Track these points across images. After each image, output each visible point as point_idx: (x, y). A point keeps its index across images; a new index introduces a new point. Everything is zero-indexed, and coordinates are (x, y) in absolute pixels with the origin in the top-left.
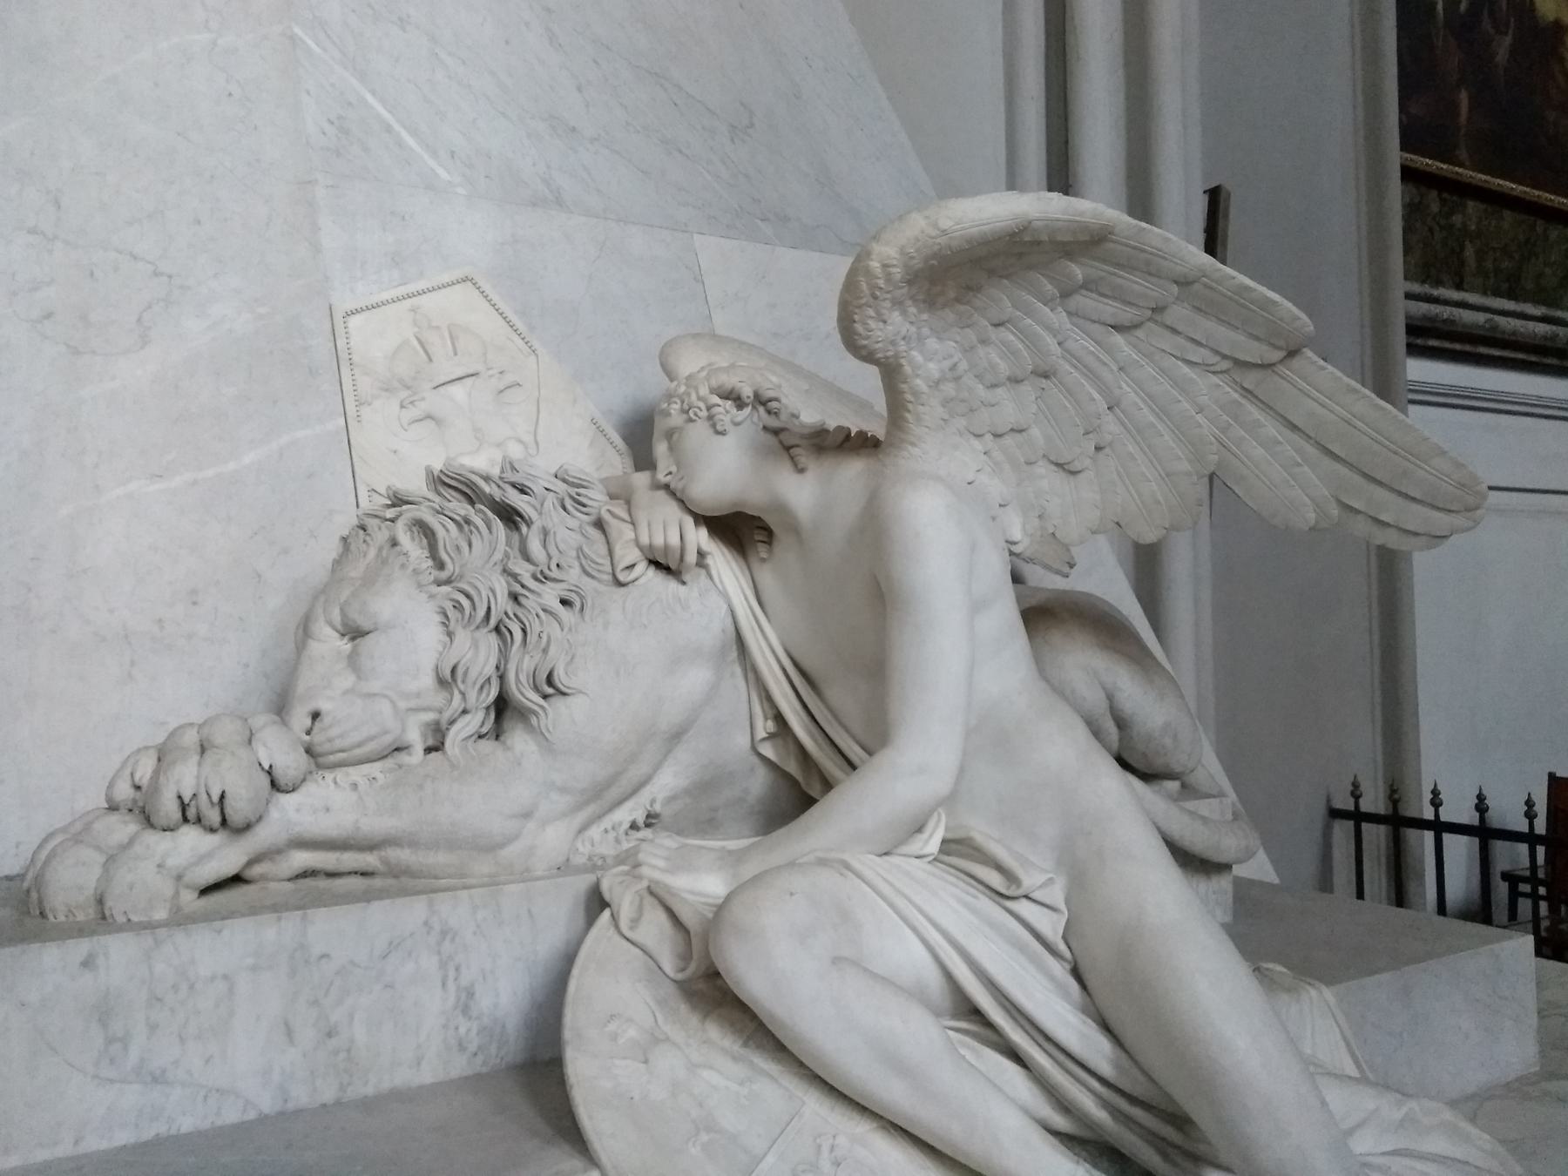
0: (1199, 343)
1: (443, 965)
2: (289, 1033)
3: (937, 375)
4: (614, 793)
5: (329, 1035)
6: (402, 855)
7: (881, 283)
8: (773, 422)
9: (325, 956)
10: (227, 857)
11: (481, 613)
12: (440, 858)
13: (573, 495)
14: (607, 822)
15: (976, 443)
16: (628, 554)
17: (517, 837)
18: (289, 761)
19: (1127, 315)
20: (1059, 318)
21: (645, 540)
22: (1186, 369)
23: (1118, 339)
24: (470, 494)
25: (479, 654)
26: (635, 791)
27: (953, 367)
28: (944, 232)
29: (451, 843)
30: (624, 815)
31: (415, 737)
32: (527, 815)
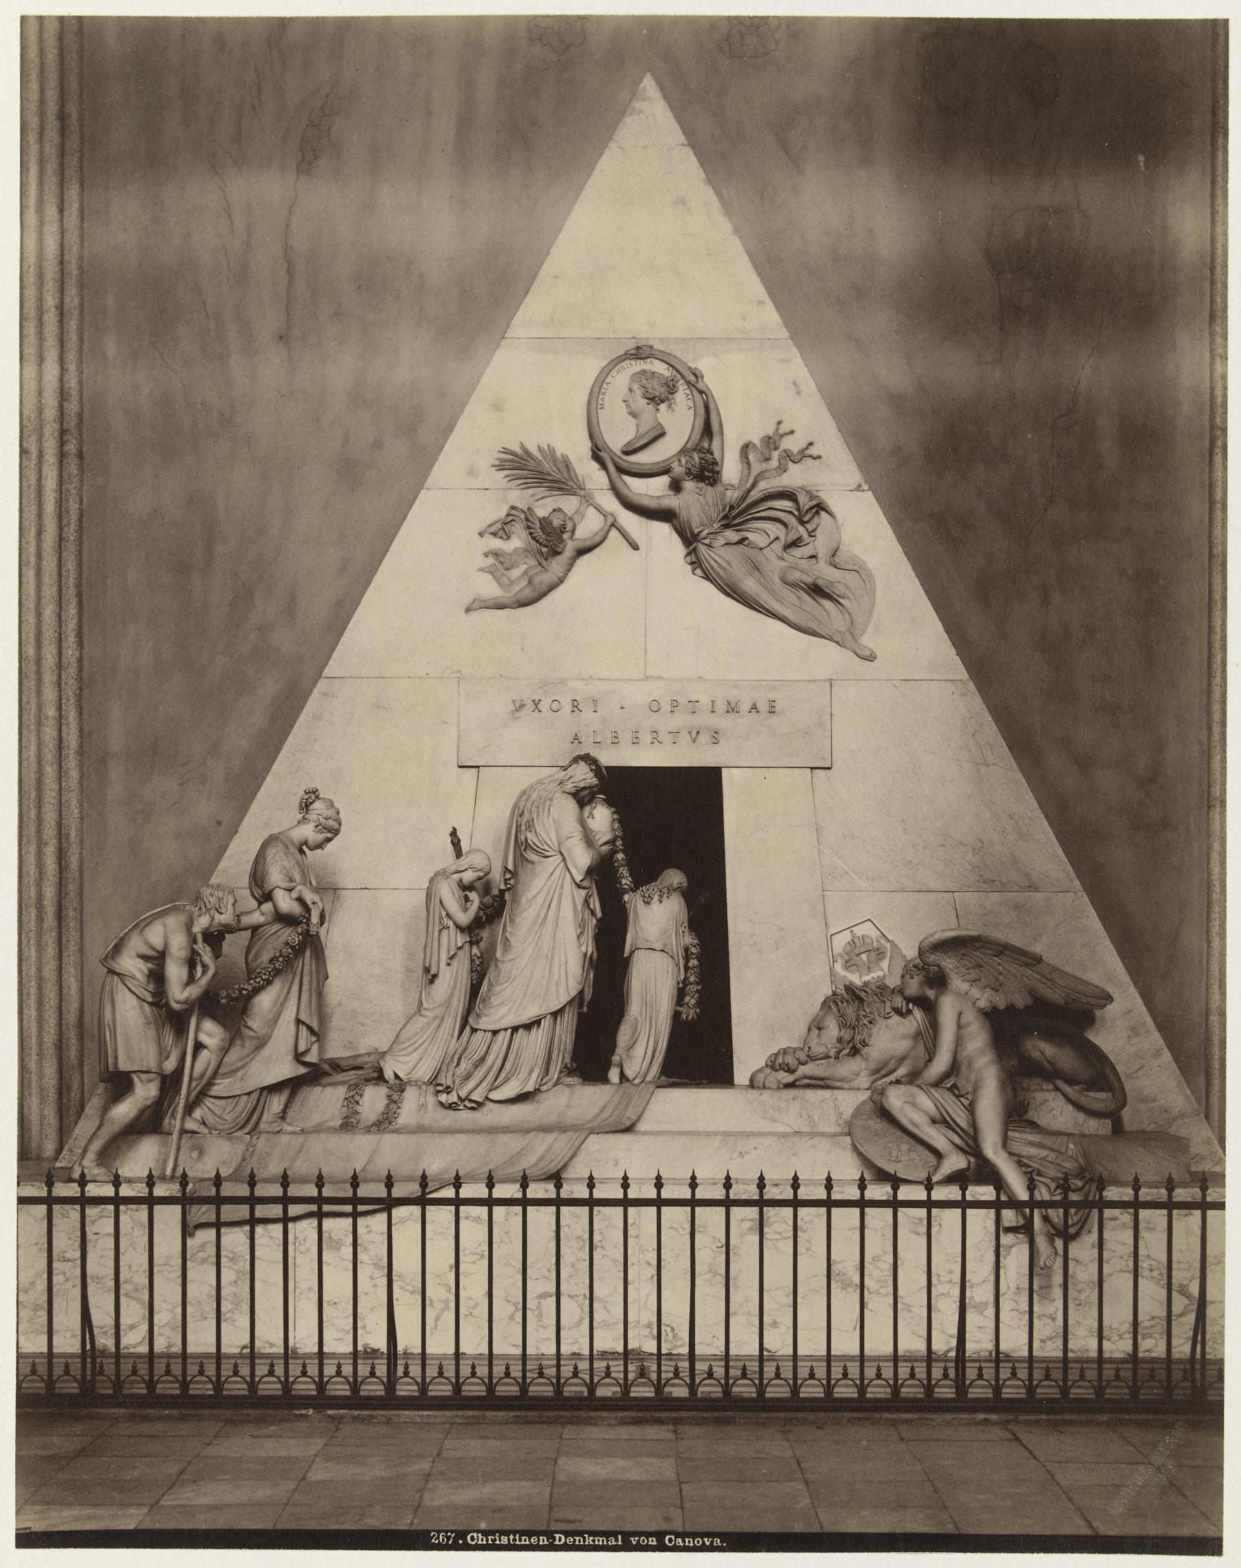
4: (883, 1072)
6: (828, 1082)
12: (838, 1084)
13: (882, 990)
16: (888, 1010)
18: (802, 1056)
24: (853, 991)
25: (846, 1035)
26: (891, 1072)
29: (841, 1080)
30: (887, 1079)
31: (832, 1053)
32: (858, 1075)
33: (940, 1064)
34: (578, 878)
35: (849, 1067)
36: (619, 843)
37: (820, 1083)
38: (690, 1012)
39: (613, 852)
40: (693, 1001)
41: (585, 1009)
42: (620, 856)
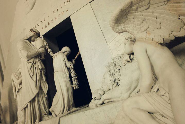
0: (160, 3)
1: (117, 110)
2: (105, 117)
3: (132, 28)
5: (109, 117)
7: (112, 26)
8: (131, 40)
9: (106, 110)
10: (101, 102)
11: (112, 74)
12: (115, 100)
14: (134, 91)
15: (144, 32)
17: (121, 96)
18: (101, 93)
19: (146, 7)
20: (139, 13)
21: (125, 60)
22: (161, 7)
23: (148, 10)
27: (133, 26)
28: (114, 17)
32: (121, 94)
33: (147, 80)
34: (26, 60)
35: (116, 93)
36: (47, 47)
37: (111, 101)
38: (75, 86)
39: (46, 50)
40: (75, 82)
41: (46, 96)
42: (49, 50)
